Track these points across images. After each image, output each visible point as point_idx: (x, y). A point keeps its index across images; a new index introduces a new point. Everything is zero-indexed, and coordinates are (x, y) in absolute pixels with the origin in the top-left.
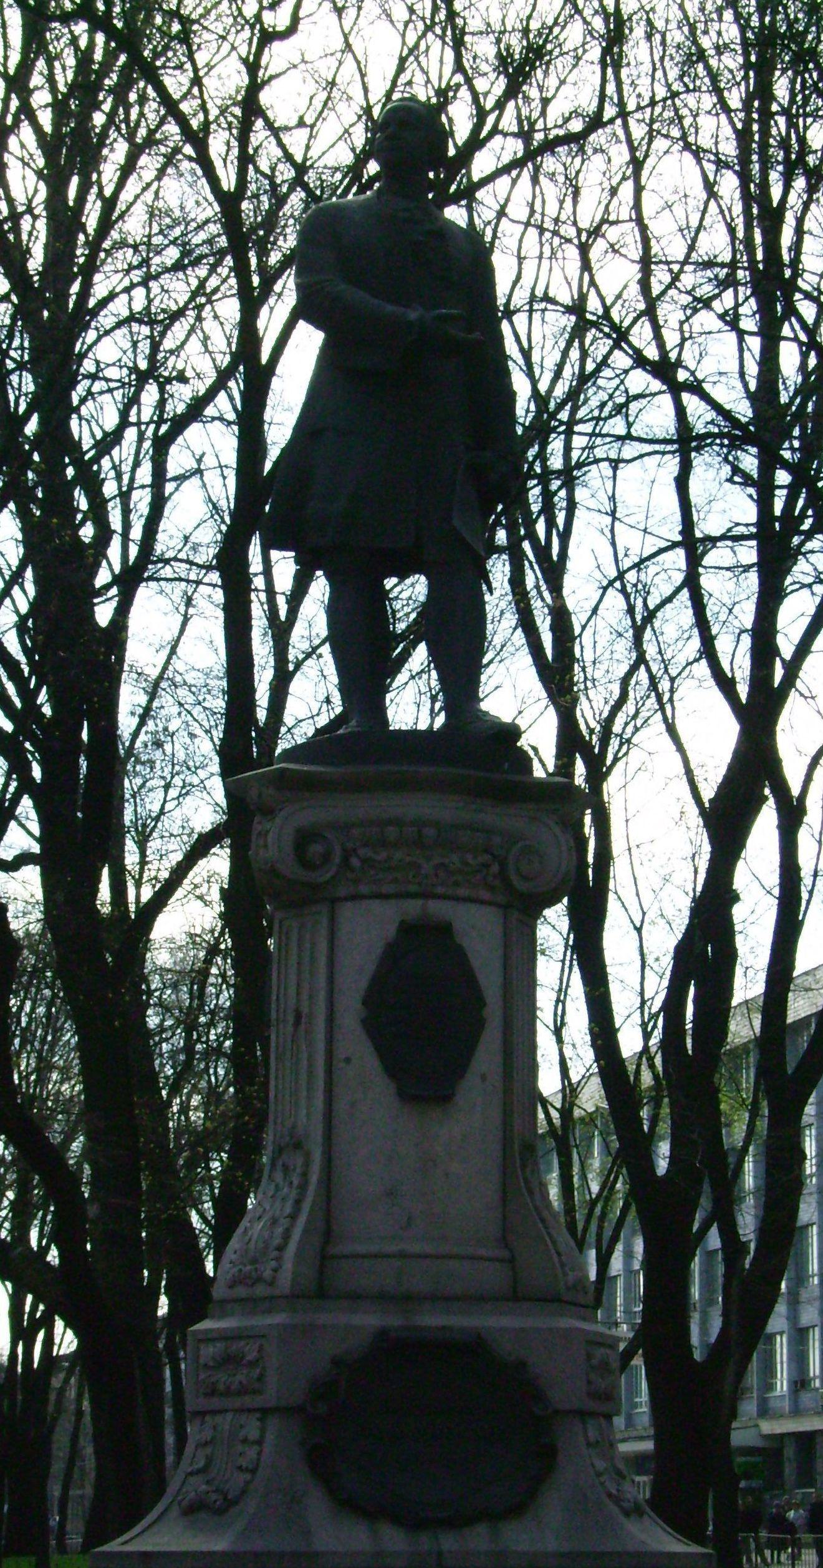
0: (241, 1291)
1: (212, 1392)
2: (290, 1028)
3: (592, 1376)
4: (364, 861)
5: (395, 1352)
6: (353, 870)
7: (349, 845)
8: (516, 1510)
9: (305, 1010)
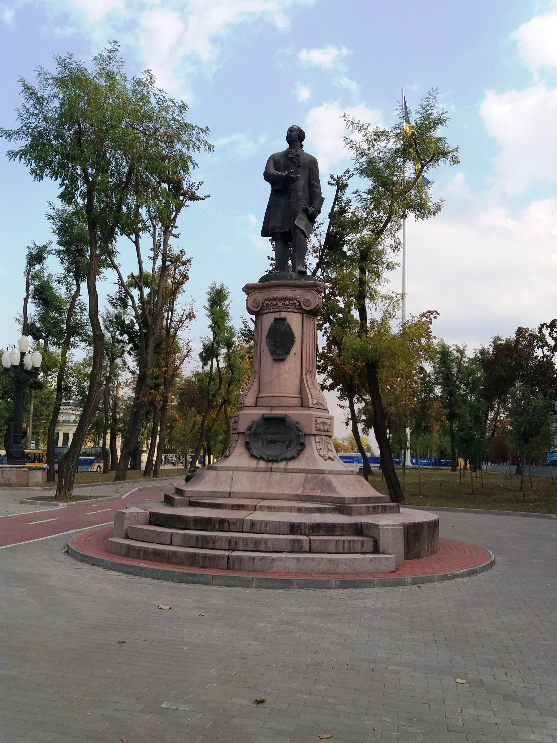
3: (317, 426)
4: (267, 304)
5: (267, 420)
8: (293, 458)
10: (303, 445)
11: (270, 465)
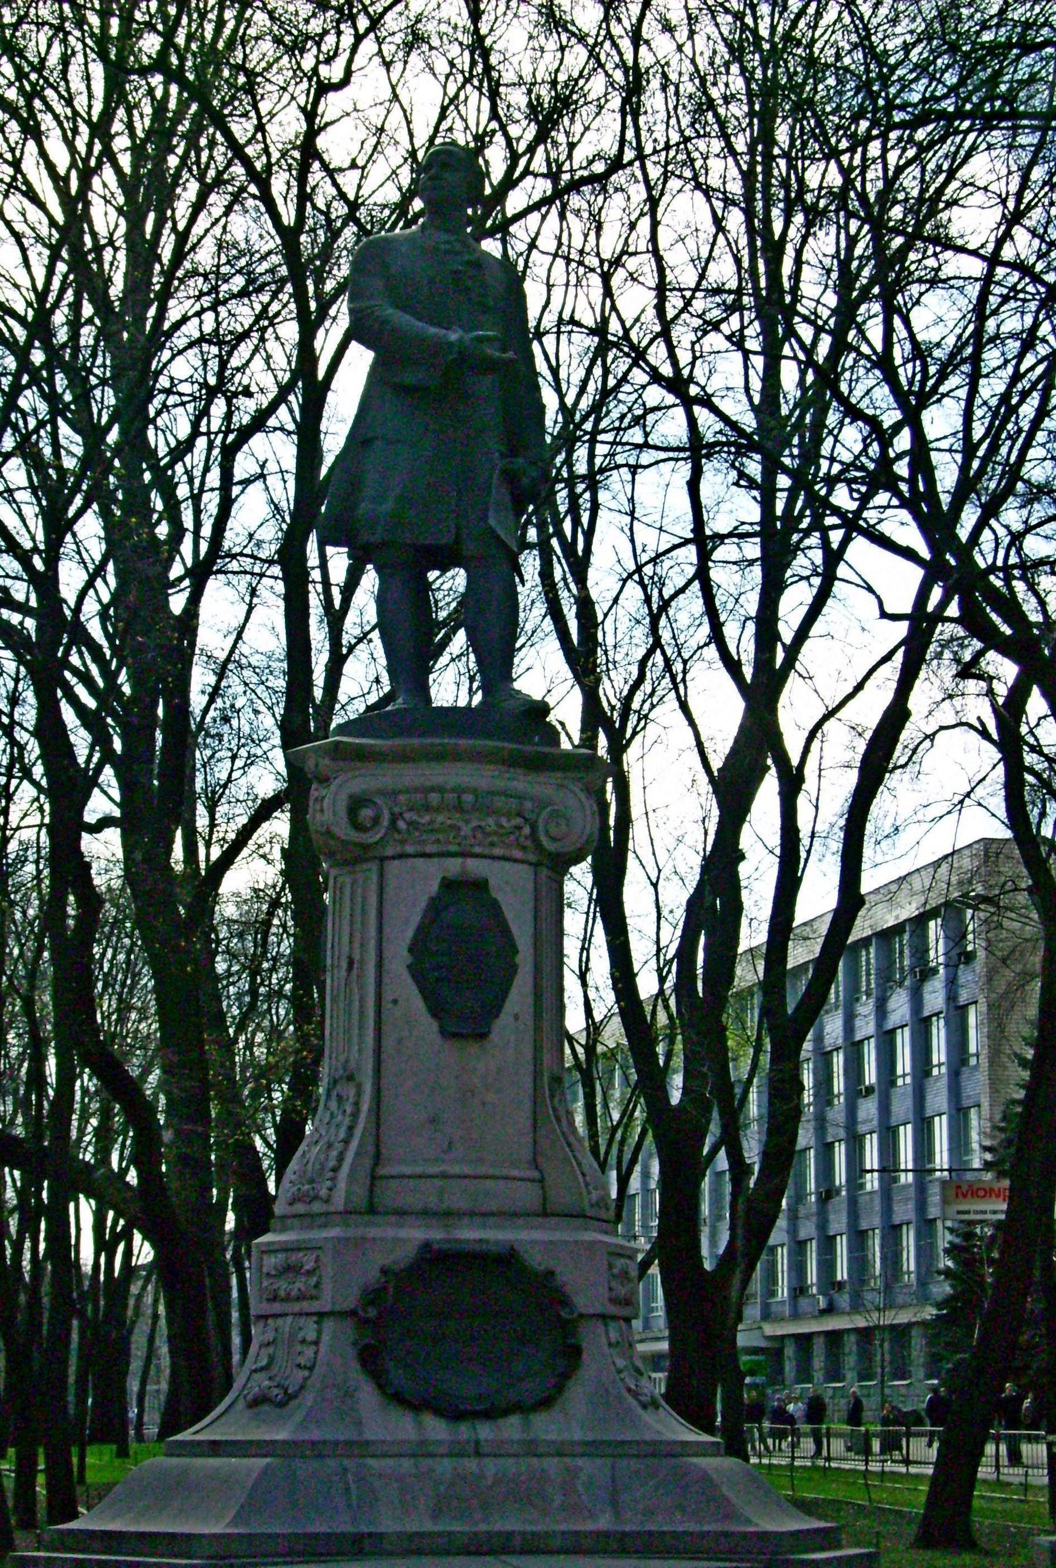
0: (300, 1208)
1: (275, 1298)
2: (344, 973)
3: (614, 1284)
5: (435, 1260)
6: (399, 832)
7: (397, 810)
8: (545, 1403)
9: (357, 957)
10: (575, 1353)
11: (464, 1431)
